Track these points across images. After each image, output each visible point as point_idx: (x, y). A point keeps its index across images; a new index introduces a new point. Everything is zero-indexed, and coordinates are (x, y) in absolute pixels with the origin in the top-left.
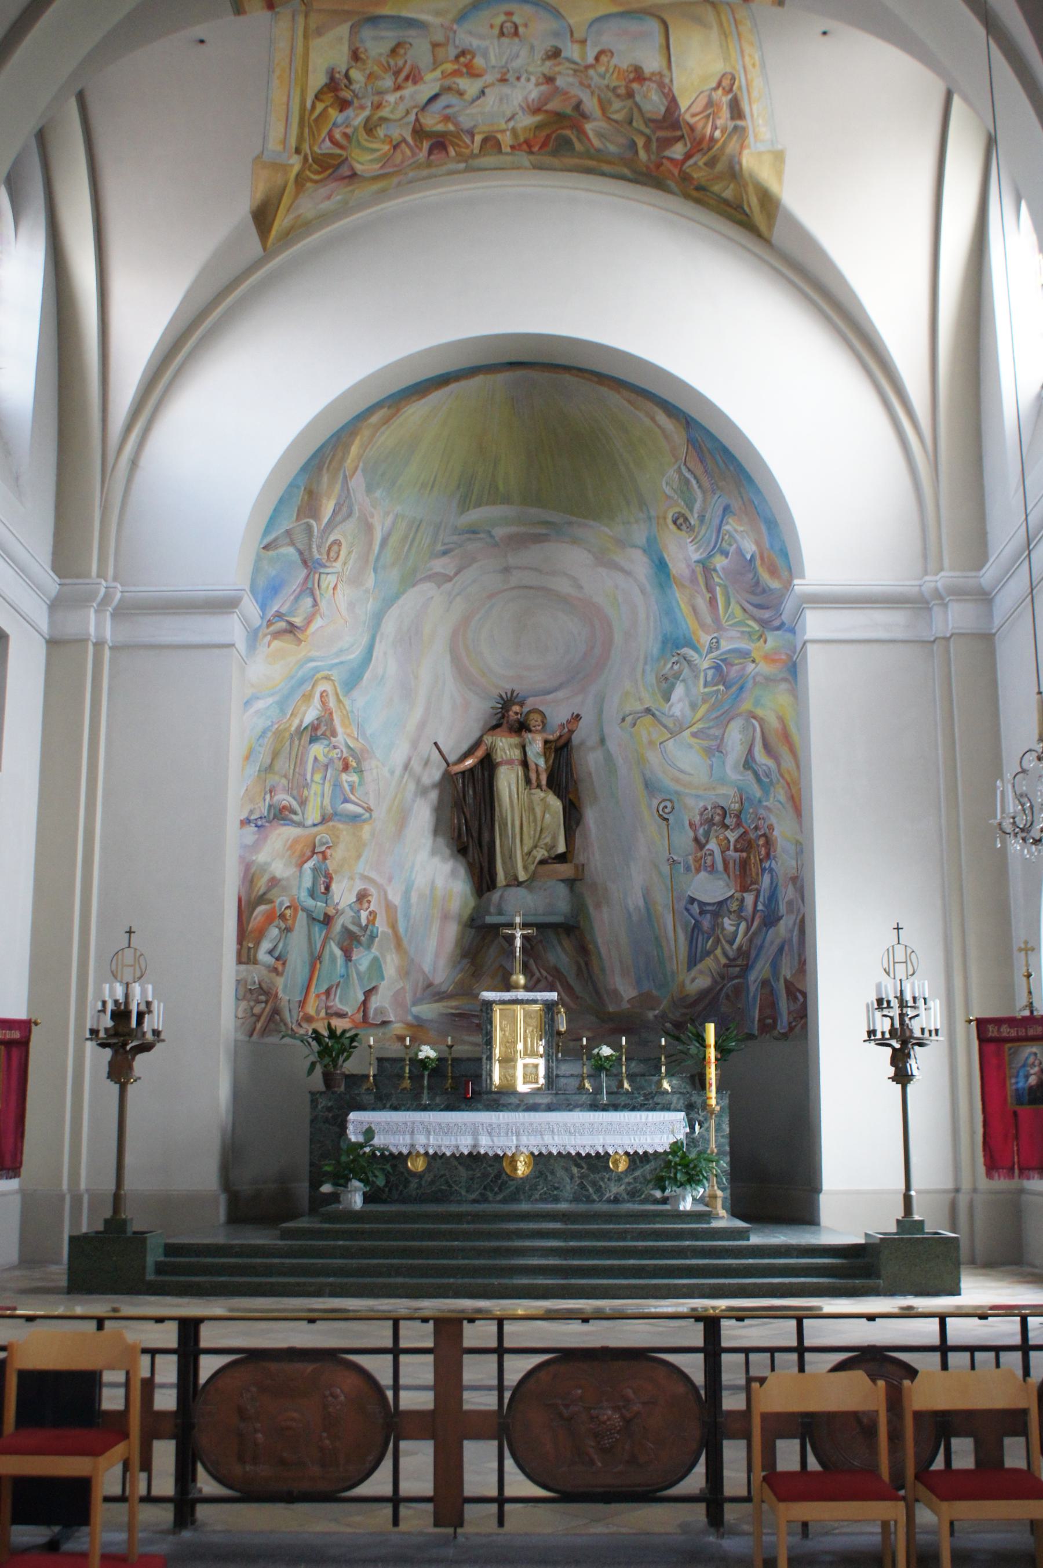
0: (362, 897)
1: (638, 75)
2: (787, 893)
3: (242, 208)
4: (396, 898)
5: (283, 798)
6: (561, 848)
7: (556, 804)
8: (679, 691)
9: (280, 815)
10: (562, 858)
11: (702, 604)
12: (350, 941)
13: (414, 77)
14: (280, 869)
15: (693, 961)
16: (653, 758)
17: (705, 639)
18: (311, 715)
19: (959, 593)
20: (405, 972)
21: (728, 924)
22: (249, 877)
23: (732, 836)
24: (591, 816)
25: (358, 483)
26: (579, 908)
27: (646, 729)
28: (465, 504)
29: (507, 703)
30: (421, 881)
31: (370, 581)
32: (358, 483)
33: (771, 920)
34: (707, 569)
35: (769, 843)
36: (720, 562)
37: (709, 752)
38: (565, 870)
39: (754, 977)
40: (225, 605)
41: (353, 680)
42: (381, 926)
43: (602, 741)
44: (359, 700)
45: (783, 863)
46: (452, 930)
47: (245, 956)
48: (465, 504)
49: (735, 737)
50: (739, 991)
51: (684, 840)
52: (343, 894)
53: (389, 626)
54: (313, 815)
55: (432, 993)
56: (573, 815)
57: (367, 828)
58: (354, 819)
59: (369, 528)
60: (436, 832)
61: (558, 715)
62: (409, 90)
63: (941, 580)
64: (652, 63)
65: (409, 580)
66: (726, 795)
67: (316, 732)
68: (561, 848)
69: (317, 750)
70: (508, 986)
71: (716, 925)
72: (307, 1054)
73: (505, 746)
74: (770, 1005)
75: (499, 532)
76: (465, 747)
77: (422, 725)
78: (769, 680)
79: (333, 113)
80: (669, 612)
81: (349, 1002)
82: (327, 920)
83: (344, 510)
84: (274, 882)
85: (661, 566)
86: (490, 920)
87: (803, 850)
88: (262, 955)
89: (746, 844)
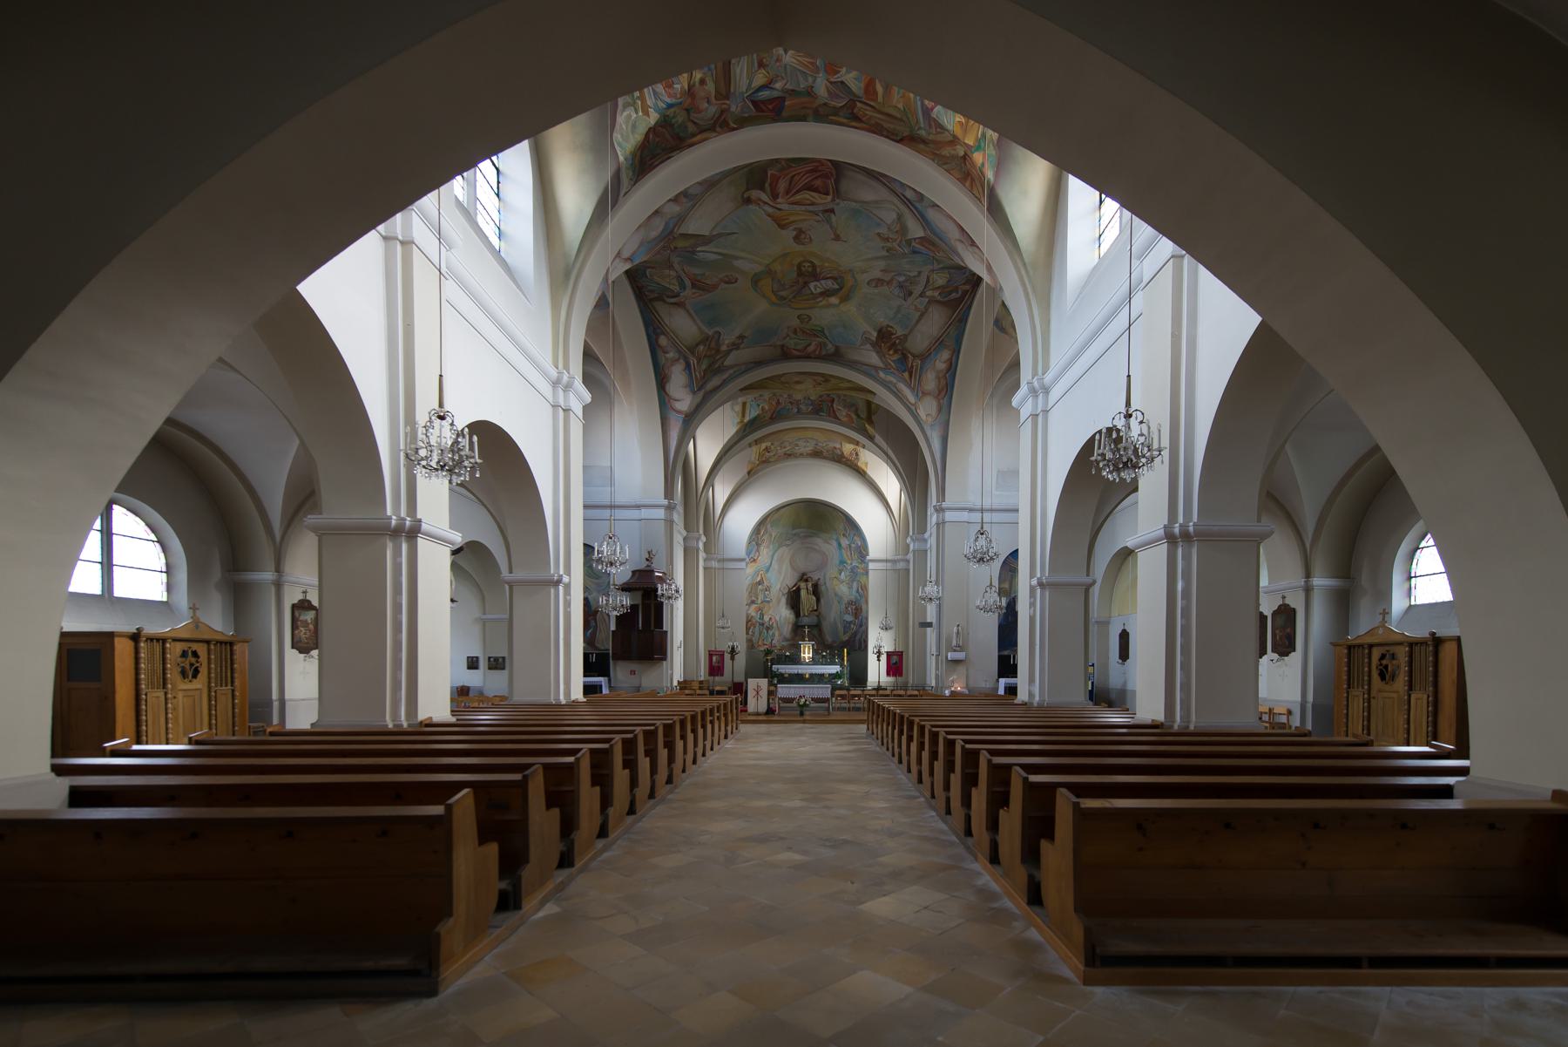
0: (770, 619)
1: (835, 448)
2: (864, 621)
3: (746, 471)
4: (778, 619)
5: (753, 598)
6: (815, 608)
7: (814, 598)
8: (843, 573)
9: (753, 602)
10: (816, 611)
11: (849, 554)
12: (768, 629)
13: (785, 447)
14: (753, 614)
15: (844, 634)
16: (837, 588)
17: (849, 562)
18: (759, 579)
19: (902, 560)
20: (780, 635)
21: (852, 626)
22: (748, 617)
23: (854, 607)
24: (822, 601)
25: (769, 526)
26: (819, 621)
27: (835, 582)
28: (794, 528)
29: (804, 574)
30: (783, 615)
31: (771, 546)
32: (769, 526)
33: (861, 626)
34: (850, 547)
35: (861, 609)
36: (853, 545)
37: (849, 588)
38: (815, 613)
39: (857, 638)
40: (743, 560)
41: (768, 570)
42: (775, 625)
43: (825, 583)
44: (769, 575)
45: (864, 614)
46: (790, 626)
47: (747, 633)
48: (794, 528)
49: (855, 584)
50: (854, 641)
51: (843, 606)
52: (766, 618)
53: (775, 558)
54: (759, 601)
55: (786, 639)
56: (818, 600)
57: (771, 604)
58: (768, 602)
59: (771, 535)
60: (787, 604)
61: (815, 578)
62: (784, 450)
63: (899, 557)
64: (838, 446)
65: (780, 546)
66: (853, 598)
67: (760, 583)
68: (815, 608)
69: (760, 587)
70: (804, 641)
71: (850, 626)
72: (762, 655)
73: (803, 585)
74: (860, 643)
75: (802, 535)
76: (792, 585)
77: (784, 579)
78: (863, 574)
79: (767, 454)
80: (841, 555)
81: (768, 642)
82: (763, 624)
83: (766, 531)
84: (752, 617)
85: (839, 544)
86: (800, 624)
87: (867, 612)
88: (750, 633)
89: (856, 609)
